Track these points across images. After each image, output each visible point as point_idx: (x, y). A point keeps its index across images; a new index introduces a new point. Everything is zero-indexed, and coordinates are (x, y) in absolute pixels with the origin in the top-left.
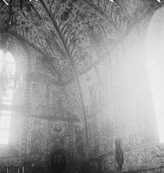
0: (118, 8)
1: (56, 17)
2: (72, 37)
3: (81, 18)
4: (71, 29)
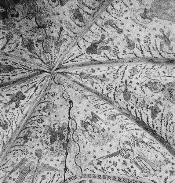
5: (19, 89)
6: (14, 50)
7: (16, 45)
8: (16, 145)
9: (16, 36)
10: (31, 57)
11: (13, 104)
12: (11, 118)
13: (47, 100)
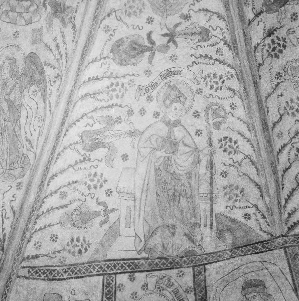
2: (97, 127)
4: (115, 101)
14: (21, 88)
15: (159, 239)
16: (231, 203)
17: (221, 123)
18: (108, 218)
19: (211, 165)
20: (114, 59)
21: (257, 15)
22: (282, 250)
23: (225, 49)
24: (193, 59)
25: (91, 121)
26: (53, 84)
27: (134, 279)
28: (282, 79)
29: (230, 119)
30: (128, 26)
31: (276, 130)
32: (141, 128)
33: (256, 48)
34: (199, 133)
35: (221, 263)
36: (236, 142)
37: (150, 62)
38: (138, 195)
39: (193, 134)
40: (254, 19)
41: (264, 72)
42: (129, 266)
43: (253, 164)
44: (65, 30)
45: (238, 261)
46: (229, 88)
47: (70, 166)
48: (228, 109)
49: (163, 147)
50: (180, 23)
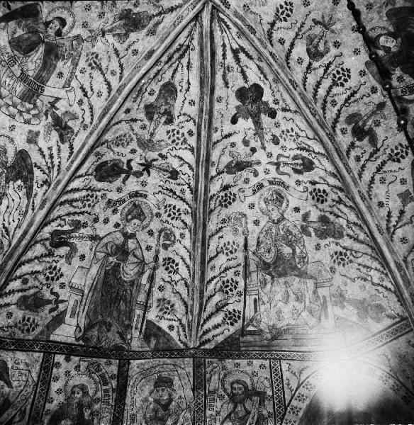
0: (237, 283)
1: (98, 154)
2: (66, 228)
3: (130, 212)
4: (87, 209)
5: (230, 92)
6: (121, 66)
7: (113, 56)
8: (364, 166)
9: (100, 47)
10: (152, 32)
11: (265, 119)
12: (294, 140)
13: (289, 36)
14: (7, 178)
15: (97, 332)
16: (161, 314)
17: (169, 245)
18: (58, 307)
19: (152, 278)
20: (95, 177)
21: (219, 174)
22: (191, 360)
23: (188, 191)
24: (160, 189)
25: (63, 223)
26: (39, 185)
27: (70, 360)
28: (226, 225)
29: (177, 245)
30: (114, 153)
31: (211, 264)
32: (102, 234)
33: (212, 197)
34: (149, 248)
35: (143, 361)
36: (177, 265)
37: (124, 182)
38: (86, 292)
39: (144, 248)
40: (216, 176)
41: (214, 218)
42: (67, 349)
43: (186, 286)
44: (62, 146)
45: (156, 361)
46: (183, 221)
47: (36, 258)
48: (178, 237)
49: (116, 254)
50: (157, 160)
